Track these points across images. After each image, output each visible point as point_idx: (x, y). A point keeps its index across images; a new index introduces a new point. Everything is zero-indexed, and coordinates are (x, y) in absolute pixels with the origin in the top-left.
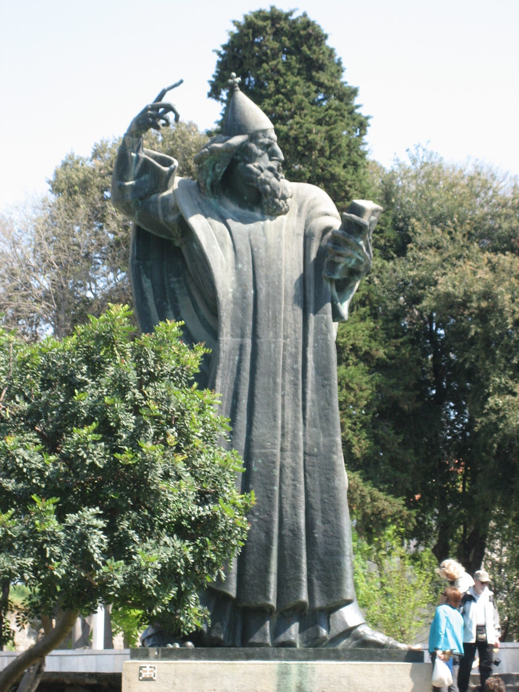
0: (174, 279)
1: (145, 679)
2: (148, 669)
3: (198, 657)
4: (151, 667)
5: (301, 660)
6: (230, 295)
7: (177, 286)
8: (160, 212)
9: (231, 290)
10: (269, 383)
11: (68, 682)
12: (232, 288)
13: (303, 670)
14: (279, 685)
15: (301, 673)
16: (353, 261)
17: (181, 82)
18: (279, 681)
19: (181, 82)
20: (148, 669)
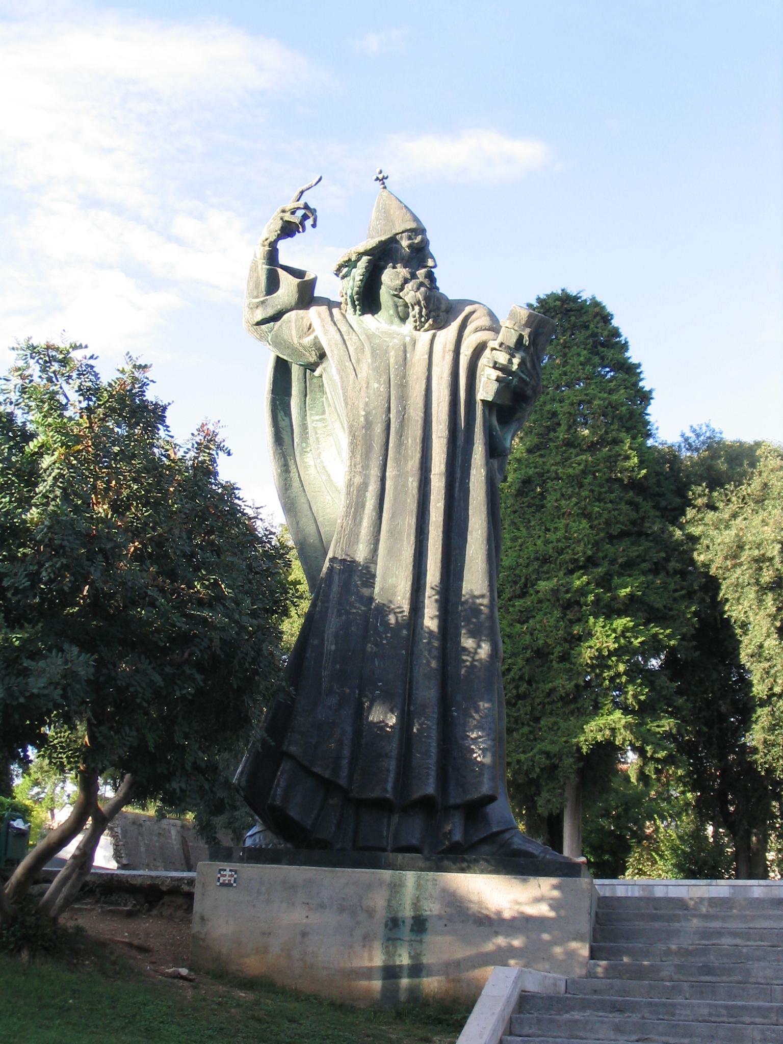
0: (317, 418)
1: (223, 885)
2: (228, 873)
3: (293, 861)
4: (231, 870)
5: (422, 870)
6: (362, 419)
7: (320, 424)
8: (294, 333)
9: (363, 413)
10: (404, 523)
11: (164, 888)
12: (364, 410)
13: (422, 882)
14: (389, 901)
15: (419, 886)
16: (515, 381)
17: (320, 180)
18: (391, 895)
19: (320, 180)
20: (228, 873)
